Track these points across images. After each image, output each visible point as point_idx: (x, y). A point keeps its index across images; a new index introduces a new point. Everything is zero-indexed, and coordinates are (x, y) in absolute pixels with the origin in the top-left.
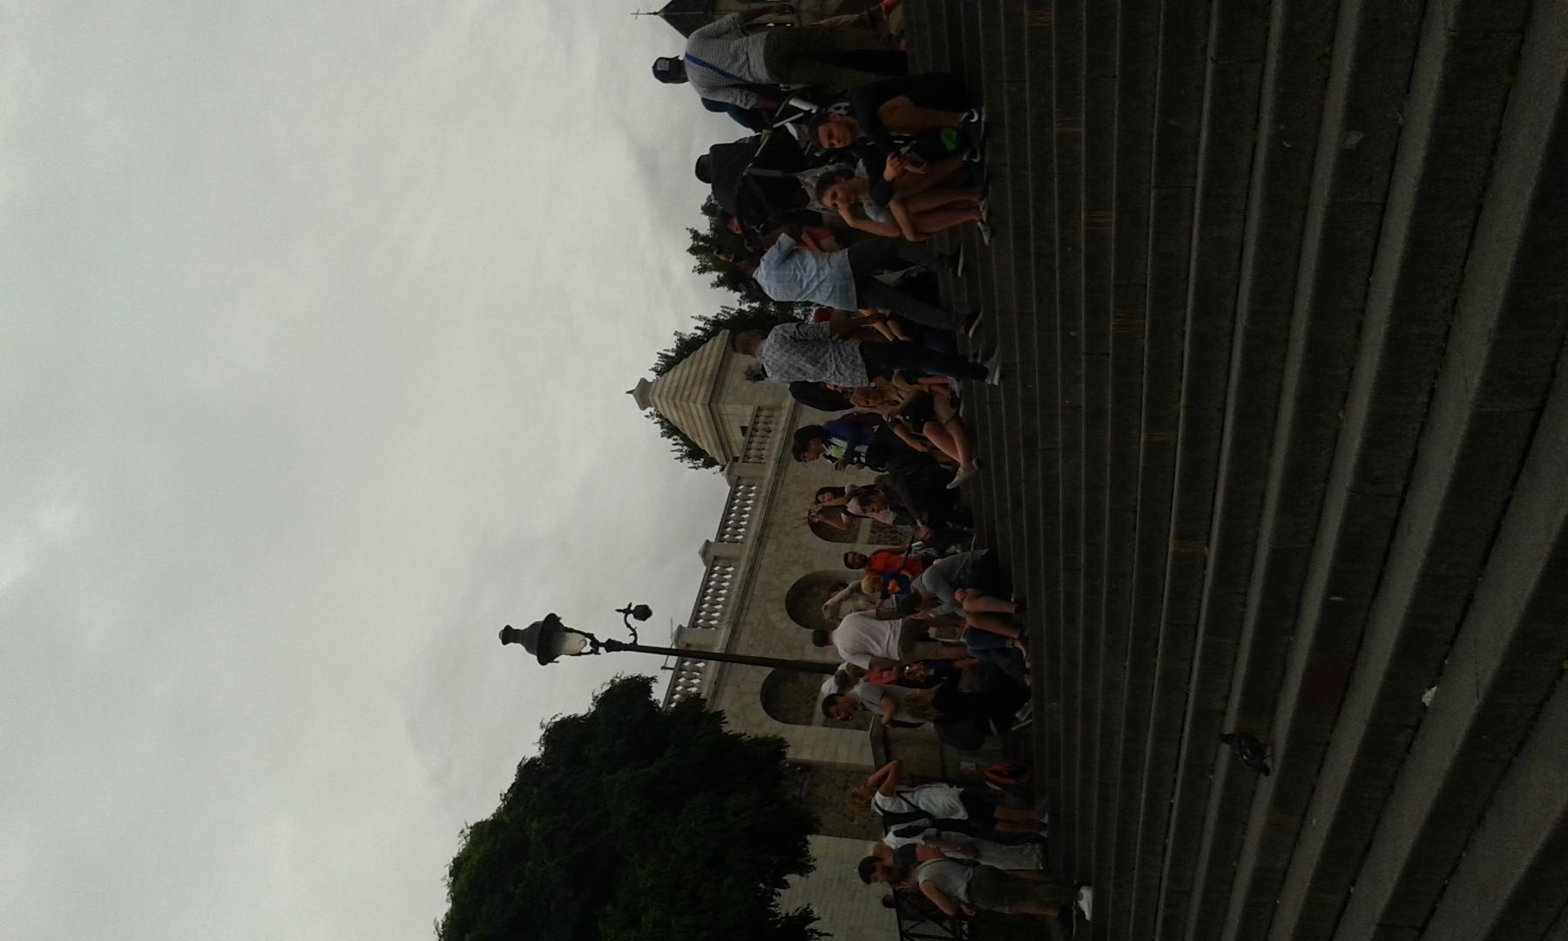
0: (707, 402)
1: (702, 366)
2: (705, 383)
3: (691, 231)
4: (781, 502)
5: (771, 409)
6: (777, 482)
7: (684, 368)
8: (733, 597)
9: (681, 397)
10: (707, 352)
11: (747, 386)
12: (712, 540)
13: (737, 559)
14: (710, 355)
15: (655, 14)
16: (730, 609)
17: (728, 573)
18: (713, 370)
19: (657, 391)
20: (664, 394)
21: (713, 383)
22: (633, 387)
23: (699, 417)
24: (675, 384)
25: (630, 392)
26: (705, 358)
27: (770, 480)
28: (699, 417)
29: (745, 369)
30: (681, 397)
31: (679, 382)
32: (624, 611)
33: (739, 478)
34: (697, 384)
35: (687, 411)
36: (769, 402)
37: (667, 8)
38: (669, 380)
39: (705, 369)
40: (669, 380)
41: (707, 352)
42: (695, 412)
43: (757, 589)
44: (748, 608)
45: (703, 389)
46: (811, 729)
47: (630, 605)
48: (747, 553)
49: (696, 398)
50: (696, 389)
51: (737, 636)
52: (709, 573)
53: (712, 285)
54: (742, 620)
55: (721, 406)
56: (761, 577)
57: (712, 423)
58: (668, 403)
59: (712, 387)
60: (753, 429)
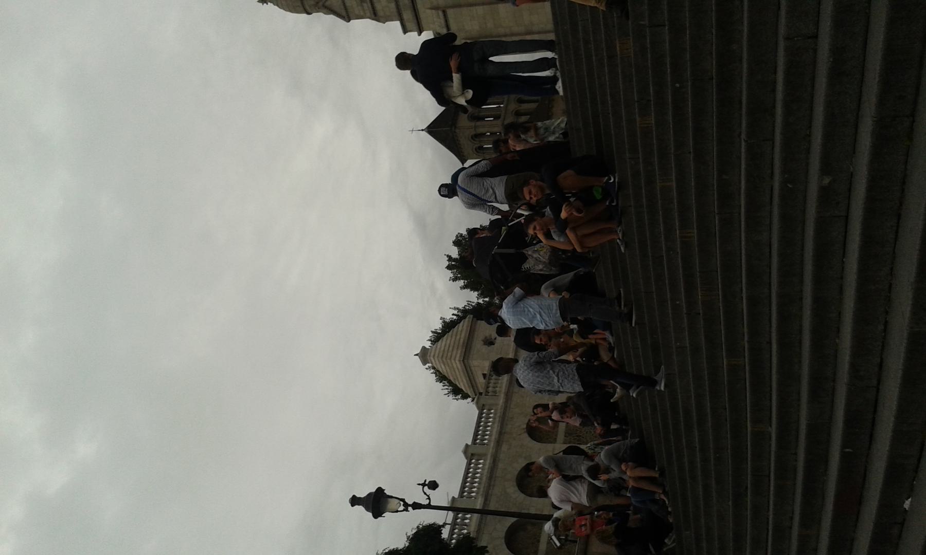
0: (462, 360)
1: (458, 337)
2: (460, 348)
3: (448, 256)
7: (447, 340)
8: (484, 478)
10: (460, 329)
11: (485, 349)
12: (470, 443)
14: (461, 331)
15: (422, 130)
16: (483, 485)
17: (480, 464)
19: (432, 354)
20: (436, 355)
21: (465, 347)
22: (418, 351)
23: (458, 369)
24: (442, 349)
26: (459, 333)
28: (458, 369)
30: (446, 357)
32: (422, 485)
33: (483, 405)
35: (450, 365)
37: (429, 127)
38: (439, 347)
39: (460, 338)
40: (439, 347)
41: (460, 329)
42: (455, 366)
44: (494, 486)
45: (459, 352)
47: (425, 481)
48: (491, 450)
50: (455, 352)
52: (469, 464)
53: (461, 288)
54: (490, 492)
55: (470, 361)
56: (500, 465)
57: (465, 372)
58: (439, 361)
59: (464, 350)
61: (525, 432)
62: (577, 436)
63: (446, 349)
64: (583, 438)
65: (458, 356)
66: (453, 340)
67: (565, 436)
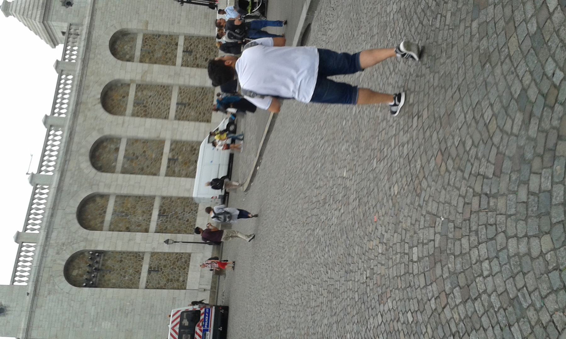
5: (76, 25)
6: (82, 74)
8: (61, 152)
9: (27, 15)
20: (18, 11)
23: (38, 27)
24: (23, 6)
27: (79, 73)
28: (38, 27)
30: (27, 15)
31: (25, 5)
33: (62, 71)
34: (35, 7)
35: (31, 22)
36: (75, 21)
42: (35, 24)
43: (74, 147)
44: (69, 160)
45: (39, 12)
48: (68, 124)
51: (63, 178)
55: (49, 22)
56: (76, 139)
57: (45, 30)
59: (44, 11)
60: (69, 34)
61: (99, 103)
63: (27, 6)
65: (38, 16)
67: (134, 106)
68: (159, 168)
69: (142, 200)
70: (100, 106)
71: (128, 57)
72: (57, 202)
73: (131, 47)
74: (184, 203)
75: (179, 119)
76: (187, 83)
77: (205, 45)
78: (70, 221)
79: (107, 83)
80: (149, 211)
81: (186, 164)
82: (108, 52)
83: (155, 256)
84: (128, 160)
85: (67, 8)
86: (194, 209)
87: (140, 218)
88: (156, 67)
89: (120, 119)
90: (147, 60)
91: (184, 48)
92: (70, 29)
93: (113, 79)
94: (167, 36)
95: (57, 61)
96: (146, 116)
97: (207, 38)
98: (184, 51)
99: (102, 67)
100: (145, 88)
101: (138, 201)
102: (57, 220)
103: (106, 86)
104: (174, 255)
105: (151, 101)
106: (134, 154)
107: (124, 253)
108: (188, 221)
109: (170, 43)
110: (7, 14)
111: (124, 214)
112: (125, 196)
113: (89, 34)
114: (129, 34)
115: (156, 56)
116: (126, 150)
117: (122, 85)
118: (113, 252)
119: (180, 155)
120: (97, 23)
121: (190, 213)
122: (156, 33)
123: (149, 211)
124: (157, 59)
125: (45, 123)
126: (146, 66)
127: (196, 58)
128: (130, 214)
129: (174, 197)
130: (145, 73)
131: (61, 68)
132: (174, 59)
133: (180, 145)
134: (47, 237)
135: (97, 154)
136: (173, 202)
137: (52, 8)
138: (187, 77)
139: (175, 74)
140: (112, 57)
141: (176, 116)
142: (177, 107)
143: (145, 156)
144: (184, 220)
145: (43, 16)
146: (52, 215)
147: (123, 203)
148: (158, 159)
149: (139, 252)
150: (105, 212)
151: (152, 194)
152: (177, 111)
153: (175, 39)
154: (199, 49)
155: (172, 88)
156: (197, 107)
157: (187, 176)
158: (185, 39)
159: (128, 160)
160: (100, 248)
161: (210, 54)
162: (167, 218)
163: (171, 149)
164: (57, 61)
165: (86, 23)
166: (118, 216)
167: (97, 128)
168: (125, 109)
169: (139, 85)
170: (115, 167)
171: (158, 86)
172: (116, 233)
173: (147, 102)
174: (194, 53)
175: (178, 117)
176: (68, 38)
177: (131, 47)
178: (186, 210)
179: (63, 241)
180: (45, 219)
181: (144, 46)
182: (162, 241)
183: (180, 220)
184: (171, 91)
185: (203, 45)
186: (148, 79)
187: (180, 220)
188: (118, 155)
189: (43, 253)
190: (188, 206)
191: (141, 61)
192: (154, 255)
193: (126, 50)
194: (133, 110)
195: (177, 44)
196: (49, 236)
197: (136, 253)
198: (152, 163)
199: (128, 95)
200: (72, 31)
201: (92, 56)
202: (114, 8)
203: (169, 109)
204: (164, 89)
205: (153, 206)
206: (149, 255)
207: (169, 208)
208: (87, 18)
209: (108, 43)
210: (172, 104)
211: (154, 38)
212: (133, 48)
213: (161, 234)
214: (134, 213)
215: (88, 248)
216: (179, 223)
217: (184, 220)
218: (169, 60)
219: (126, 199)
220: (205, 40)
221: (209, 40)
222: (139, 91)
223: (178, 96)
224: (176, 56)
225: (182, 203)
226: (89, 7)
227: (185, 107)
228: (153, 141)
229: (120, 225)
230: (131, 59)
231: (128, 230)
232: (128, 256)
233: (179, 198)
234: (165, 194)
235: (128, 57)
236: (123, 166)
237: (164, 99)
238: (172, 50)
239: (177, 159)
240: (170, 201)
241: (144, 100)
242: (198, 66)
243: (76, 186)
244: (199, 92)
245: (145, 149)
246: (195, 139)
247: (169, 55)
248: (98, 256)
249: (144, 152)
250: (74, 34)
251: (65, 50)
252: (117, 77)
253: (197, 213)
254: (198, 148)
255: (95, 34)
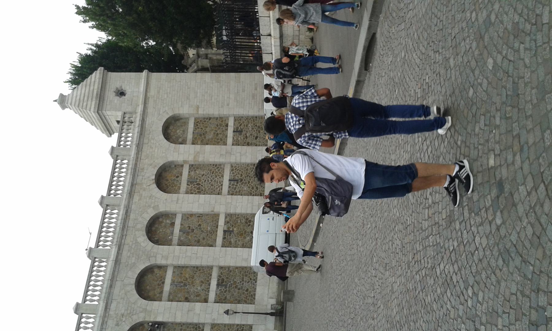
0: (96, 111)
1: (92, 88)
2: (94, 99)
4: (140, 170)
5: (131, 113)
8: (118, 228)
9: (82, 106)
10: (93, 80)
13: (119, 206)
14: (95, 82)
18: (97, 92)
19: (70, 101)
20: (73, 104)
22: (57, 97)
23: (93, 117)
24: (78, 98)
25: (55, 101)
26: (92, 84)
28: (93, 117)
29: (115, 90)
30: (82, 106)
33: (117, 156)
34: (90, 99)
35: (86, 113)
36: (129, 109)
41: (93, 80)
42: (90, 114)
43: (131, 223)
44: (126, 235)
45: (94, 103)
46: (162, 303)
49: (90, 108)
50: (89, 103)
54: (123, 241)
55: (104, 112)
56: (132, 216)
57: (101, 120)
60: (123, 122)
62: (197, 184)
63: (82, 98)
64: (202, 186)
65: (93, 106)
66: (87, 90)
67: (188, 185)
68: (215, 240)
69: (200, 270)
70: (155, 186)
71: (180, 140)
72: (116, 273)
73: (184, 131)
74: (242, 273)
75: (232, 195)
76: (238, 160)
77: (254, 124)
78: (129, 292)
79: (160, 165)
80: (208, 281)
81: (241, 235)
82: (162, 137)
83: (216, 328)
84: (184, 233)
85: (121, 97)
86: (252, 279)
87: (199, 288)
88: (208, 148)
89: (175, 196)
90: (199, 142)
91: (234, 128)
92: (124, 118)
93: (167, 161)
94: (217, 119)
95: (113, 147)
96: (199, 193)
97: (256, 117)
98: (234, 131)
99: (156, 151)
100: (198, 168)
101: (196, 271)
102: (116, 291)
103: (160, 167)
104: (235, 327)
105: (203, 179)
106: (189, 227)
107: (184, 324)
108: (247, 290)
109: (221, 125)
110: (63, 107)
111: (182, 284)
112: (183, 267)
113: (143, 121)
114: (181, 119)
115: (207, 138)
116: (181, 225)
117: (175, 166)
118: (172, 323)
119: (235, 227)
120: (150, 110)
121: (249, 282)
122: (207, 116)
123: (208, 281)
124: (208, 140)
125: (101, 203)
126: (198, 147)
127: (246, 137)
128: (189, 285)
129: (232, 267)
130: (197, 154)
131: (116, 153)
132: (224, 139)
133: (234, 218)
134: (107, 308)
135: (153, 229)
136: (231, 271)
137: (106, 99)
138: (238, 155)
139: (226, 153)
140: (165, 141)
141: (229, 192)
142: (230, 184)
143: (200, 229)
144: (244, 290)
145: (97, 106)
146: (111, 287)
147: (181, 273)
148: (214, 232)
149: (199, 324)
150: (163, 283)
151: (209, 264)
152: (229, 187)
153: (225, 120)
154: (248, 129)
155: (224, 166)
156: (249, 182)
157: (243, 246)
158: (235, 120)
159: (184, 233)
160: (160, 319)
161: (259, 132)
162: (226, 287)
163: (225, 221)
164: (113, 147)
165: (139, 111)
166: (176, 286)
167: (152, 206)
168: (179, 188)
169: (192, 165)
170: (171, 240)
171: (211, 165)
172: (175, 303)
173: (200, 180)
174: (244, 133)
175: (231, 192)
176: (123, 126)
177: (184, 131)
178: (244, 280)
179: (123, 311)
180: (104, 290)
181: (196, 129)
182: (222, 311)
183: (239, 289)
184: (224, 170)
185: (252, 124)
186: (201, 159)
187: (239, 289)
188: (173, 230)
189: (102, 324)
190: (246, 276)
191: (193, 144)
192: (215, 327)
193: (179, 134)
194: (188, 188)
195: (227, 125)
196: (108, 307)
197: (196, 324)
198: (208, 235)
199: (181, 175)
200: (126, 119)
201: (146, 141)
202: (166, 96)
203: (222, 185)
204: (216, 168)
205: (211, 275)
206: (209, 327)
207: (227, 278)
208: (140, 106)
209: (161, 129)
210: (224, 181)
211: (205, 121)
212: (185, 132)
213: (220, 304)
214: (193, 283)
215: (147, 319)
216: (238, 293)
217: (244, 290)
218: (220, 140)
219: (184, 269)
220: (254, 120)
221: (258, 119)
222: (192, 171)
223: (230, 173)
224: (226, 137)
225: (241, 272)
226: (141, 96)
227: (237, 183)
228: (208, 215)
229: (179, 295)
230: (183, 142)
231: (187, 300)
232: (188, 327)
233: (237, 268)
234: (222, 264)
235: (180, 140)
236: (179, 239)
237: (216, 176)
238: (223, 131)
239: (233, 231)
240: (228, 271)
241: (197, 179)
242: (248, 144)
243: (134, 258)
244: (251, 169)
245: (200, 223)
246: (249, 211)
247: (220, 136)
248: (157, 327)
249: (200, 225)
250: (129, 122)
251: (120, 137)
252: (170, 159)
253: (256, 282)
254: (253, 220)
255: (148, 121)
